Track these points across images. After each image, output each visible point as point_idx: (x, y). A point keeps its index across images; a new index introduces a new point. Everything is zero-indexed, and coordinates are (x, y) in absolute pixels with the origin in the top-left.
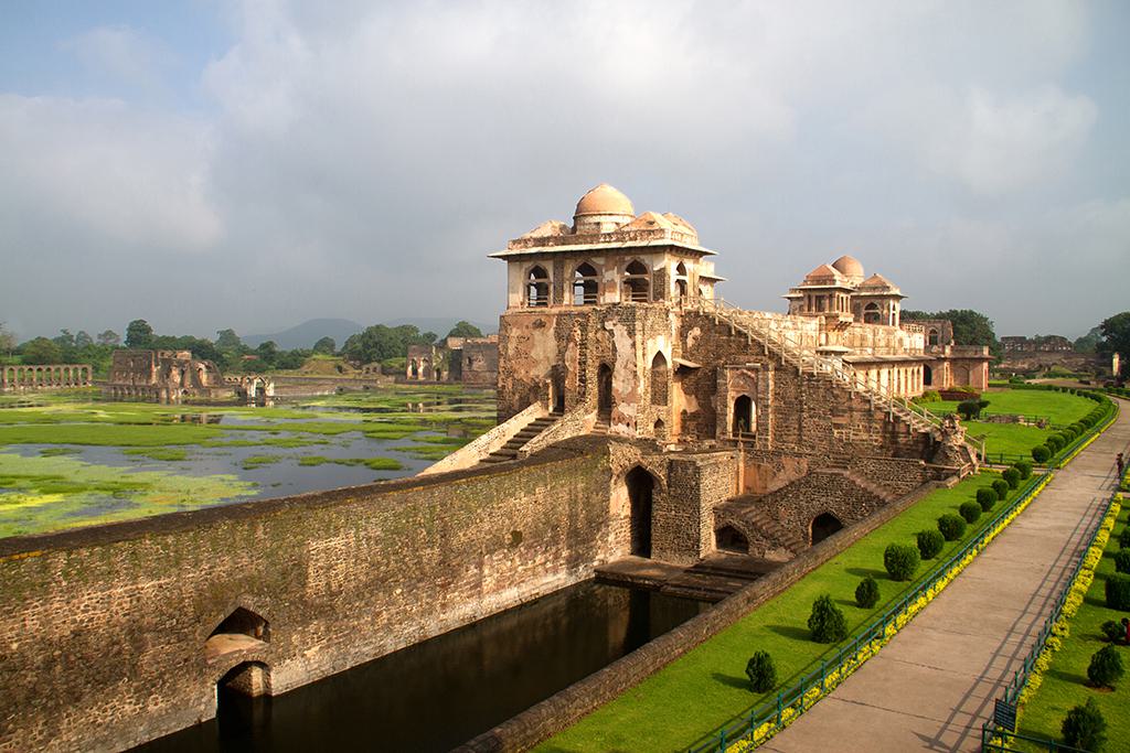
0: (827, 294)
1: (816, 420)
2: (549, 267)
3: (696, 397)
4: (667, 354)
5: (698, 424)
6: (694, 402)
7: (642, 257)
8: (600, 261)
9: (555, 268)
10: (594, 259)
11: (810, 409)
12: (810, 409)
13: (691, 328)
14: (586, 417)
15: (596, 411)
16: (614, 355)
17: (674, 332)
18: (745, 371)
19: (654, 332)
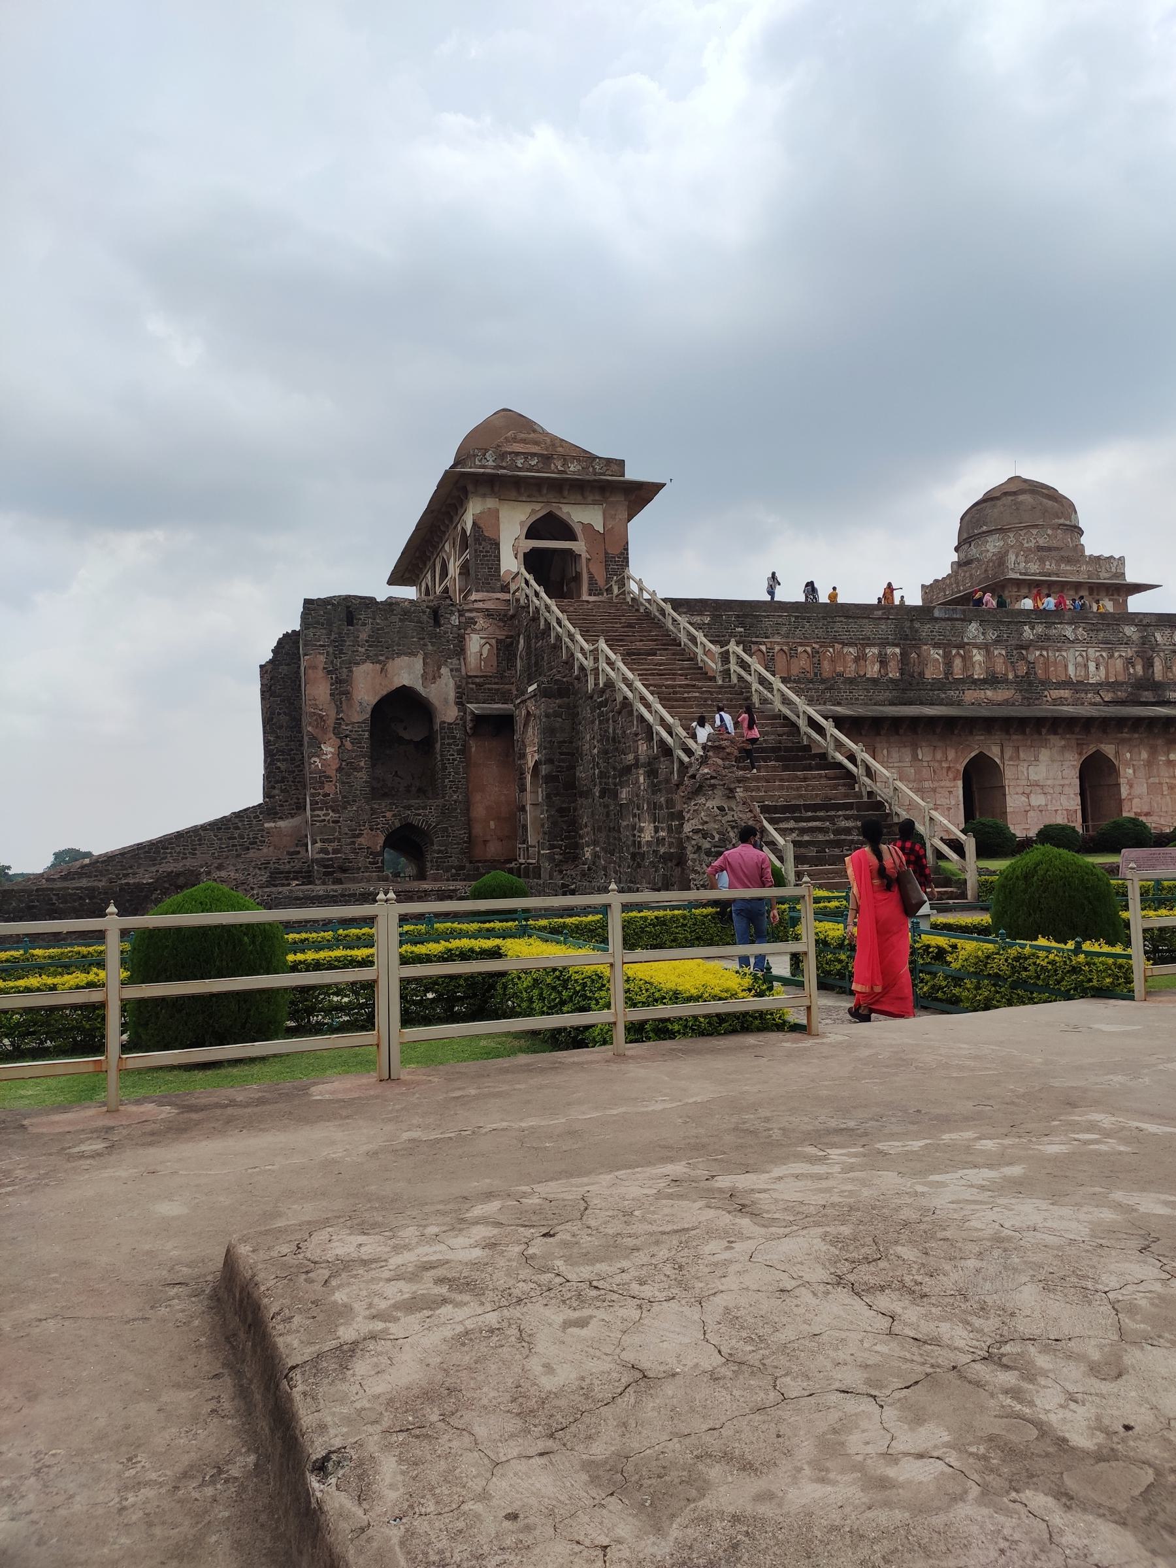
14: (266, 825)
19: (383, 650)
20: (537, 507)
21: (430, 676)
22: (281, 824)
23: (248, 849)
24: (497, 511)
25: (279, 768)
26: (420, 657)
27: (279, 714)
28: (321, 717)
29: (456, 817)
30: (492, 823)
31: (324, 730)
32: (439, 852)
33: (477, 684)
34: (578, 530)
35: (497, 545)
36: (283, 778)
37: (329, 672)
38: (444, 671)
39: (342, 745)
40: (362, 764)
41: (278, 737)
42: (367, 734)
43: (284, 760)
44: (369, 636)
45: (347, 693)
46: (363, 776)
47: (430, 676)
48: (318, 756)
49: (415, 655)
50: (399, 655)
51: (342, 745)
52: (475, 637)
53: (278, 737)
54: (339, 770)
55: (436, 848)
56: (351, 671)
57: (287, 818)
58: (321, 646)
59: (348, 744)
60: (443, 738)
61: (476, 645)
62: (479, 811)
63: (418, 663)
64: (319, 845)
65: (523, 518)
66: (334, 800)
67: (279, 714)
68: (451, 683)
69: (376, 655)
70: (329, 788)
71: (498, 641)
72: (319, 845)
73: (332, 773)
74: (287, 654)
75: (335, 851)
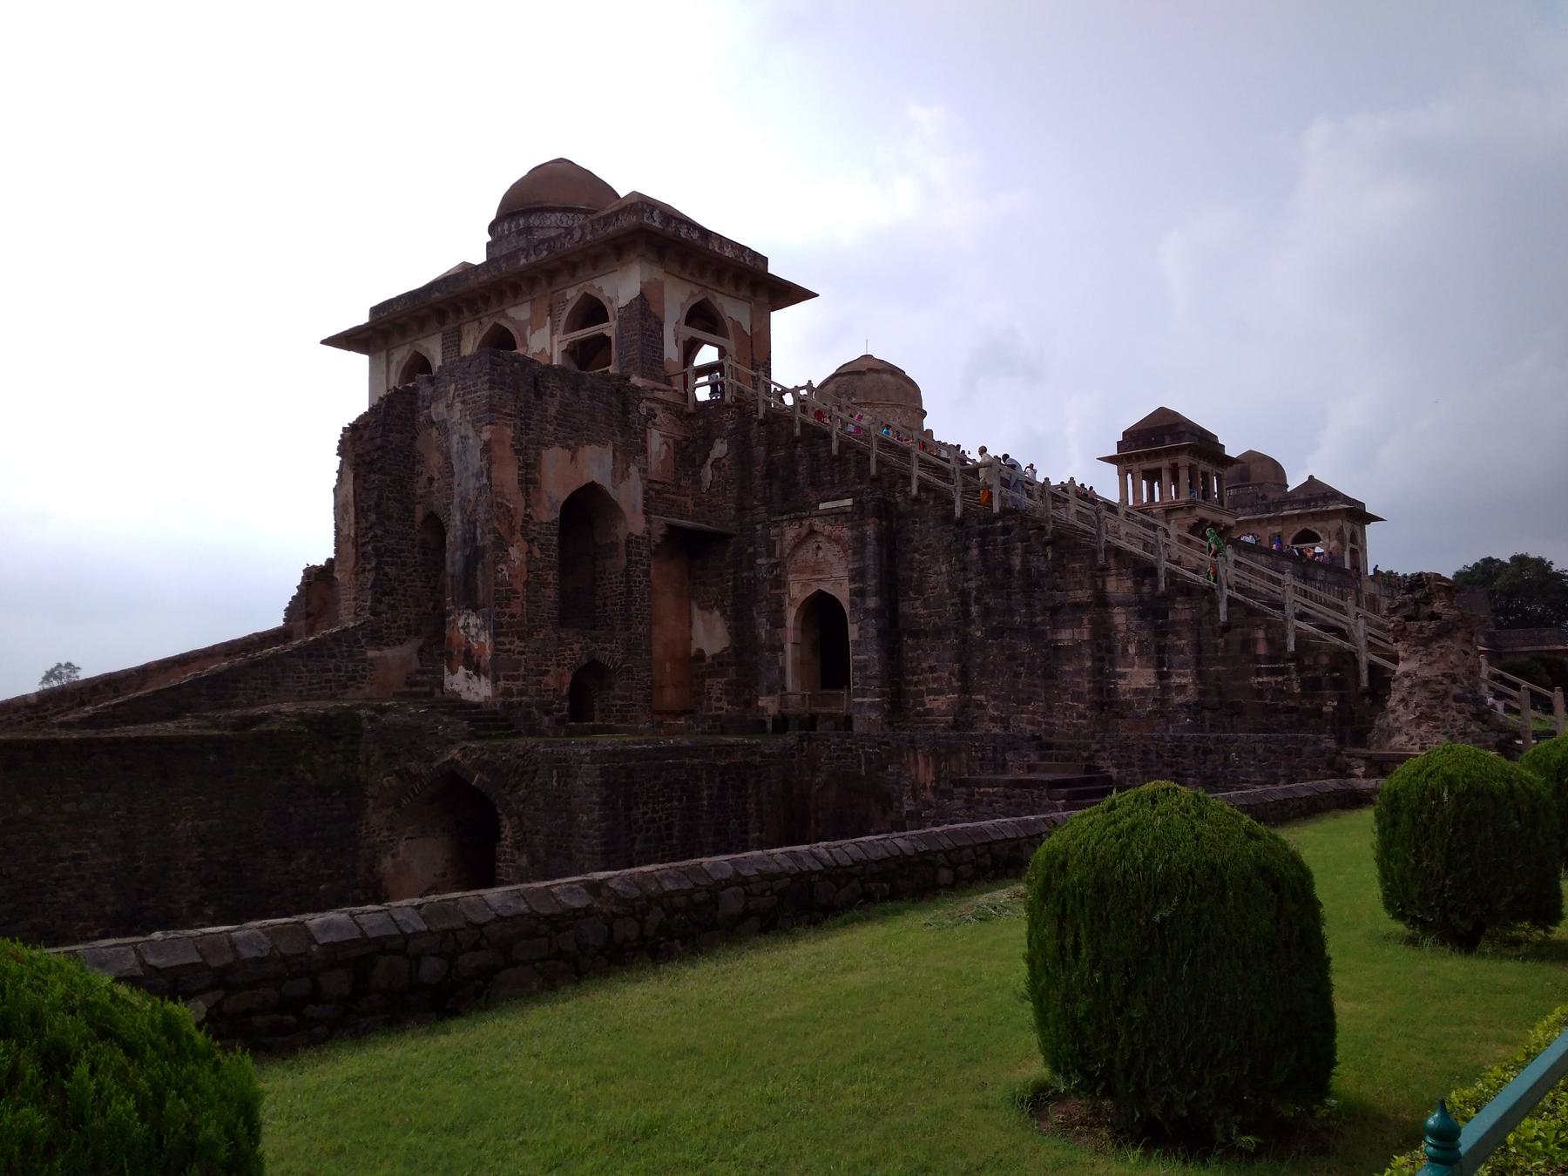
0: (1164, 464)
3: (723, 613)
4: (629, 495)
7: (598, 282)
8: (520, 313)
9: (445, 347)
12: (987, 613)
14: (371, 654)
15: (418, 642)
16: (450, 486)
17: (656, 443)
18: (818, 524)
20: (696, 289)
21: (620, 475)
22: (388, 652)
23: (346, 687)
25: (386, 574)
26: (610, 447)
30: (668, 665)
31: (513, 533)
32: (623, 698)
33: (657, 492)
34: (729, 325)
35: (661, 325)
37: (517, 452)
38: (633, 469)
39: (530, 552)
41: (386, 531)
43: (393, 564)
45: (535, 482)
46: (551, 593)
47: (619, 474)
50: (590, 441)
51: (530, 552)
52: (656, 433)
53: (386, 531)
55: (617, 691)
56: (539, 454)
59: (537, 553)
60: (629, 554)
61: (656, 443)
63: (608, 453)
65: (683, 299)
68: (640, 488)
70: (517, 608)
71: (677, 443)
72: (502, 683)
73: (519, 587)
75: (522, 693)
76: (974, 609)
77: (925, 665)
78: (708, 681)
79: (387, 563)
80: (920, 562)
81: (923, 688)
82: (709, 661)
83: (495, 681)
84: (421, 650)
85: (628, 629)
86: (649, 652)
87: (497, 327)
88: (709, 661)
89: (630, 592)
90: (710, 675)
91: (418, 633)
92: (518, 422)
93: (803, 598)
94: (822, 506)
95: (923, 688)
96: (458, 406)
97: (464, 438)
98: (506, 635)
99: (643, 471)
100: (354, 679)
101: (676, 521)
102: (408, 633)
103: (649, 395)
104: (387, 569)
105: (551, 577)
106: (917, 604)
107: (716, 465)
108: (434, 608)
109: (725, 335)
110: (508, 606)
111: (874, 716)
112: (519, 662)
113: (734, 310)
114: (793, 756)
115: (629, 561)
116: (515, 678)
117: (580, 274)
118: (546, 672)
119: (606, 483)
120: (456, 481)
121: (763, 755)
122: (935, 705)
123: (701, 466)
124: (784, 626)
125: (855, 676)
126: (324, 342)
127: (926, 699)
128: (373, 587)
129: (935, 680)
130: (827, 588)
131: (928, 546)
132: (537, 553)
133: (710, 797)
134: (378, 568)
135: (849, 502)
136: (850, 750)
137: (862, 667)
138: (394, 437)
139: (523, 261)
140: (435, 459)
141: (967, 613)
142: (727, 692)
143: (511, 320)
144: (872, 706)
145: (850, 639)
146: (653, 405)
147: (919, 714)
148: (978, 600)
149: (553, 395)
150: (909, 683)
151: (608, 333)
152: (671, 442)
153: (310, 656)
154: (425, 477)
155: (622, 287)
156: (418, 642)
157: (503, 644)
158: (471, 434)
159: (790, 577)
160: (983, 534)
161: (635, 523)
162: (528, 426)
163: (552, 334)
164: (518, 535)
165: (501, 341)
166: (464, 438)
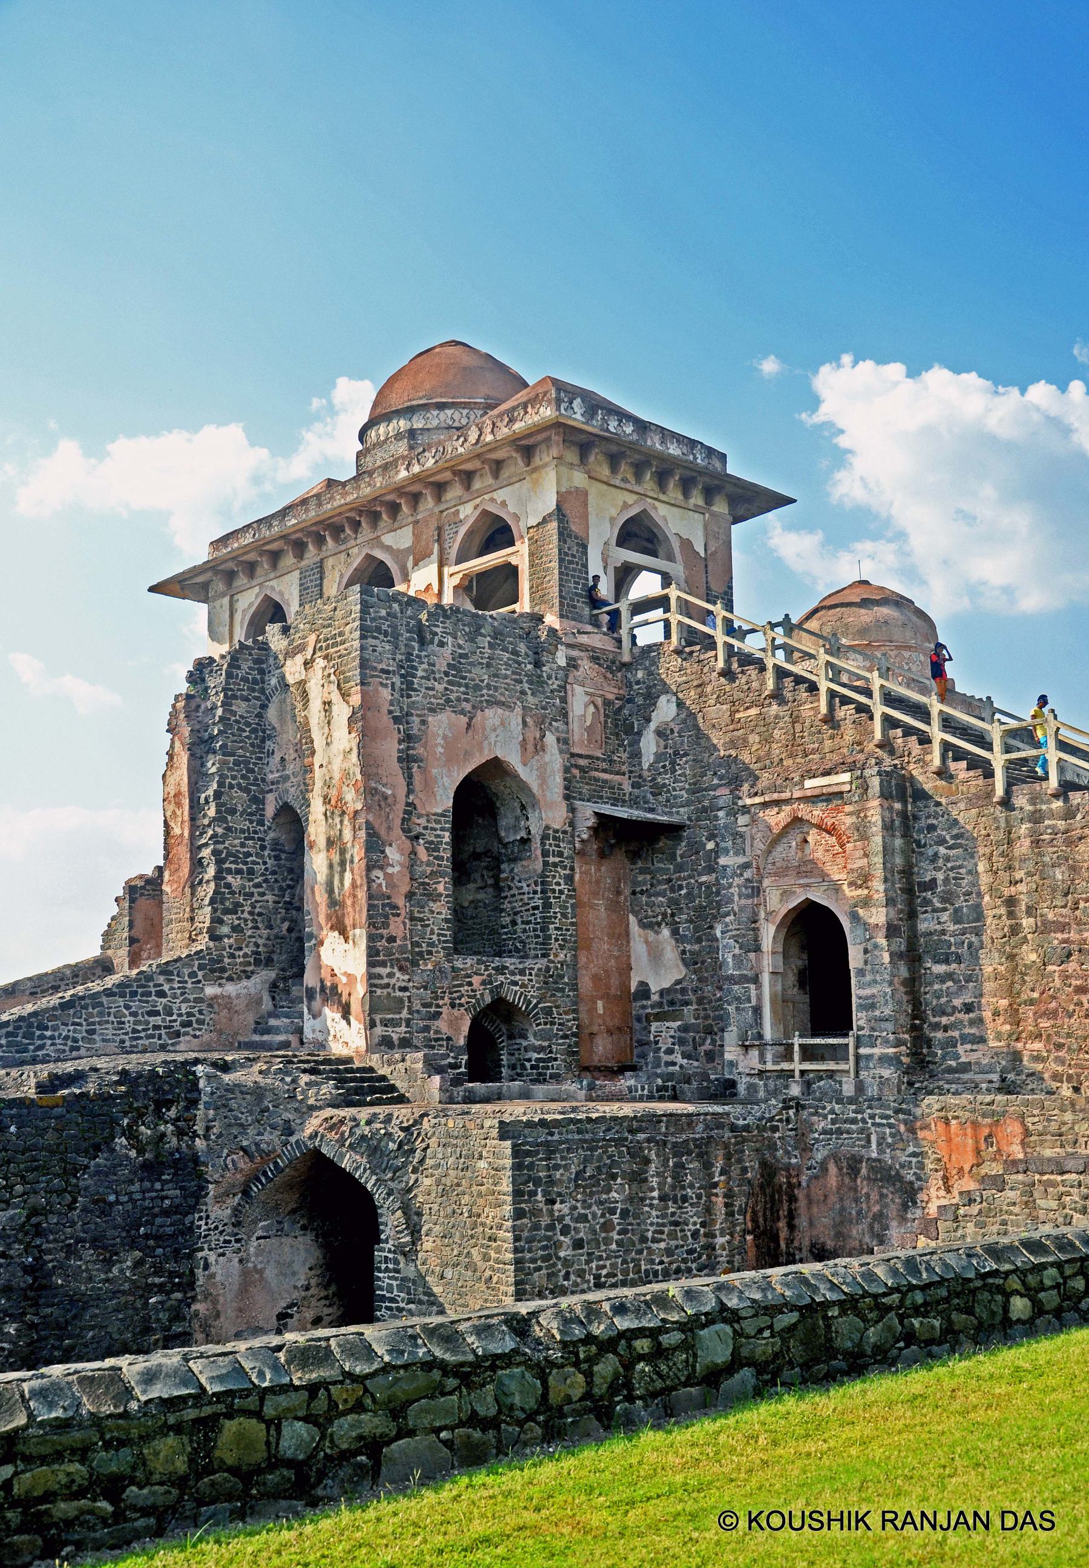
1: (1072, 966)
2: (287, 589)
3: (675, 932)
5: (684, 1029)
6: (670, 952)
7: (500, 495)
10: (388, 539)
11: (1045, 928)
12: (1045, 928)
13: (651, 699)
14: (210, 991)
15: (266, 975)
17: (581, 705)
18: (803, 811)
19: (467, 693)
20: (631, 499)
21: (534, 748)
22: (231, 989)
23: (178, 1034)
24: (586, 494)
25: (228, 886)
26: (518, 710)
27: (231, 787)
28: (385, 798)
29: (562, 990)
32: (541, 1049)
33: (582, 769)
35: (585, 547)
36: (237, 905)
37: (397, 720)
38: (550, 739)
40: (441, 888)
42: (447, 837)
43: (239, 872)
44: (449, 665)
46: (441, 910)
47: (530, 747)
48: (381, 868)
49: (510, 708)
51: (414, 852)
54: (410, 896)
55: (532, 1040)
56: (424, 722)
57: (240, 979)
58: (383, 671)
59: (423, 854)
60: (545, 854)
61: (581, 705)
62: (586, 984)
63: (515, 719)
64: (379, 1030)
65: (614, 512)
66: (402, 949)
67: (231, 787)
69: (458, 699)
70: (397, 927)
71: (607, 703)
72: (379, 1030)
73: (400, 901)
74: (245, 680)
76: (1027, 922)
77: (957, 1002)
78: (654, 1026)
79: (229, 871)
80: (947, 859)
81: (956, 1034)
82: (655, 998)
83: (372, 1025)
84: (274, 986)
85: (544, 956)
86: (574, 987)
87: (368, 556)
88: (655, 998)
89: (547, 906)
90: (659, 1017)
91: (269, 962)
92: (397, 680)
93: (783, 911)
94: (809, 783)
95: (956, 1034)
96: (320, 663)
97: (327, 704)
98: (383, 964)
99: (563, 741)
100: (189, 1024)
101: (607, 809)
102: (257, 962)
103: (570, 640)
104: (229, 879)
105: (442, 886)
106: (945, 917)
107: (659, 733)
108: (290, 930)
109: (671, 558)
110: (385, 925)
111: (886, 1073)
112: (401, 1000)
113: (679, 521)
114: (775, 1129)
115: (546, 864)
116: (395, 1023)
117: (477, 485)
118: (437, 1015)
119: (513, 759)
120: (317, 760)
121: (733, 1128)
122: (973, 1057)
123: (639, 734)
124: (758, 949)
125: (859, 1018)
126: (152, 589)
127: (960, 1049)
128: (212, 902)
129: (972, 1023)
130: (818, 896)
131: (956, 837)
132: (423, 854)
133: (661, 1185)
134: (218, 877)
135: (846, 777)
136: (854, 1121)
137: (869, 1005)
138: (240, 707)
139: (403, 474)
140: (289, 735)
141: (1015, 930)
142: (682, 1042)
143: (388, 549)
144: (883, 1060)
145: (853, 965)
146: (575, 653)
147: (950, 1070)
148: (1030, 911)
149: (442, 644)
150: (936, 1027)
151: (514, 561)
152: (599, 701)
153: (134, 994)
154: (277, 757)
155: (531, 500)
156: (266, 975)
157: (380, 977)
158: (336, 697)
159: (766, 882)
160: (1036, 818)
161: (555, 816)
162: (410, 686)
163: (441, 566)
164: (397, 831)
165: (376, 576)
166: (327, 704)
